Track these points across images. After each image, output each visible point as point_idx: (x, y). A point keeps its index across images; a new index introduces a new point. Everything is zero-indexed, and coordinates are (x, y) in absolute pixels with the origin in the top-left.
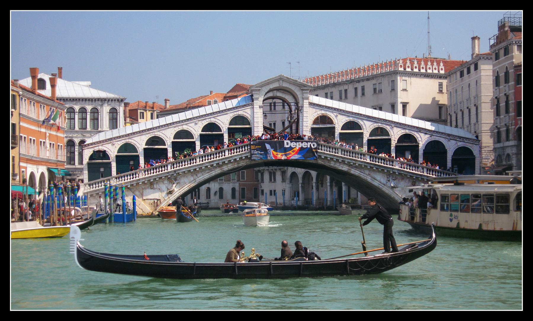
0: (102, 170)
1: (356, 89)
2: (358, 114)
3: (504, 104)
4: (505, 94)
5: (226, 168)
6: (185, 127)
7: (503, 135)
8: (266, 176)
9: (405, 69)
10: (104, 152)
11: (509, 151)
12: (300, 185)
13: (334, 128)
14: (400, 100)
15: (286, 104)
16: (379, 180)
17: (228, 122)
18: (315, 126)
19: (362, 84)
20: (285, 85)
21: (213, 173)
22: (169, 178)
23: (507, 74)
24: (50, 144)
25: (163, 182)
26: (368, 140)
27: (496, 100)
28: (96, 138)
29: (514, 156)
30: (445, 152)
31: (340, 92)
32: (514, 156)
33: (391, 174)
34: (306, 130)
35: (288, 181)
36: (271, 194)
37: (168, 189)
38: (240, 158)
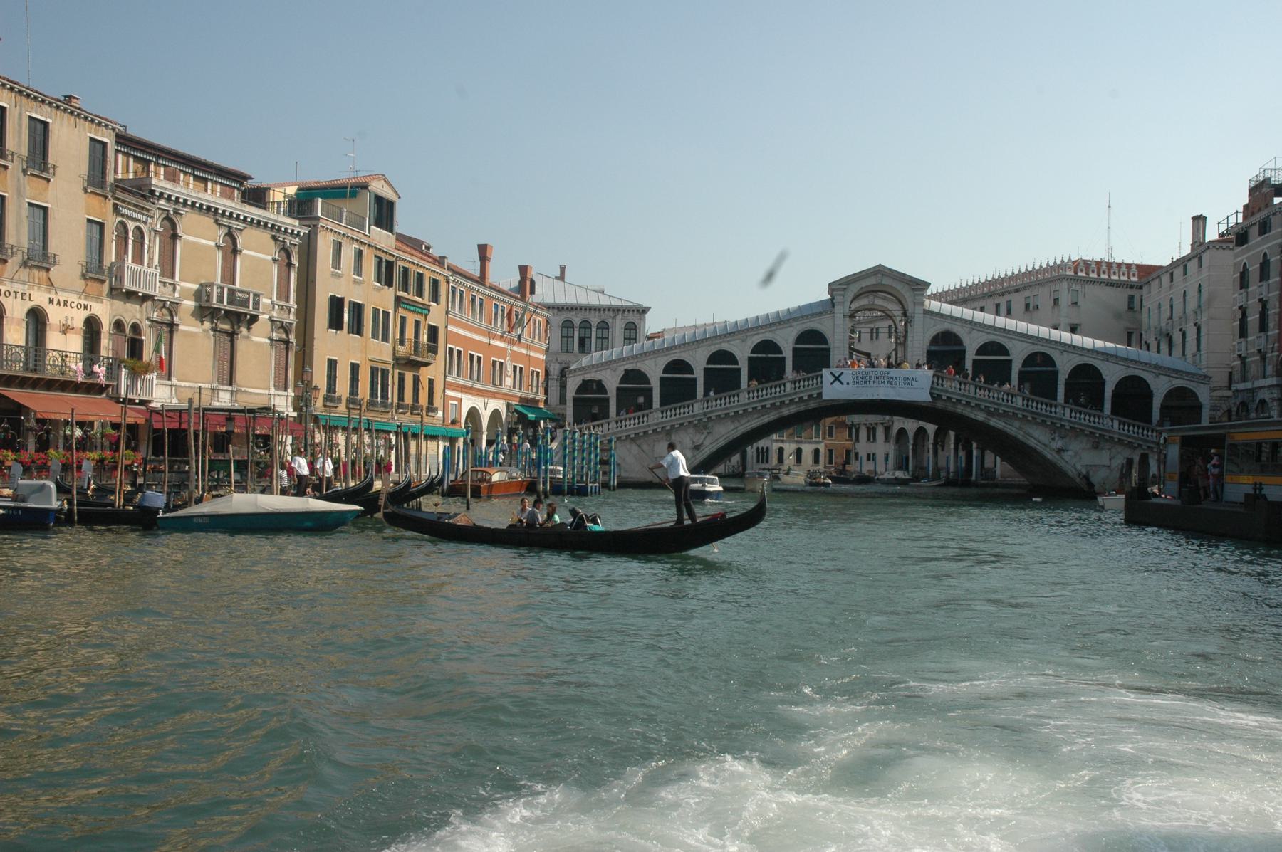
4: (1261, 300)
5: (786, 412)
6: (725, 346)
8: (863, 433)
10: (599, 383)
11: (1265, 395)
16: (1037, 438)
18: (933, 348)
19: (1007, 297)
20: (886, 281)
21: (766, 419)
22: (695, 425)
24: (515, 367)
27: (1240, 312)
28: (584, 361)
30: (1150, 395)
35: (892, 441)
36: (869, 459)
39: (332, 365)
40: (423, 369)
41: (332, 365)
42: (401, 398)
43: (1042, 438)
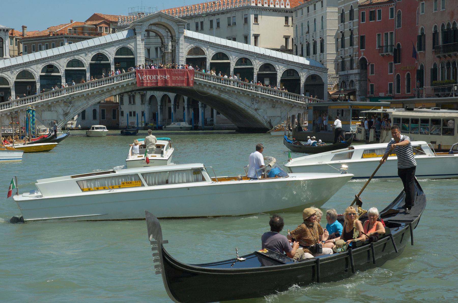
1: (211, 22)
2: (226, 46)
3: (349, 37)
4: (350, 30)
6: (77, 57)
7: (348, 64)
9: (256, 5)
11: (352, 78)
12: (159, 107)
13: (205, 58)
14: (252, 33)
16: (244, 104)
17: (114, 53)
19: (217, 17)
20: (163, 21)
22: (65, 102)
23: (351, 12)
25: (59, 105)
26: (235, 69)
29: (357, 82)
31: (197, 24)
32: (357, 82)
33: (254, 98)
34: (182, 61)
35: (147, 103)
36: (131, 115)
37: (64, 111)
38: (127, 84)
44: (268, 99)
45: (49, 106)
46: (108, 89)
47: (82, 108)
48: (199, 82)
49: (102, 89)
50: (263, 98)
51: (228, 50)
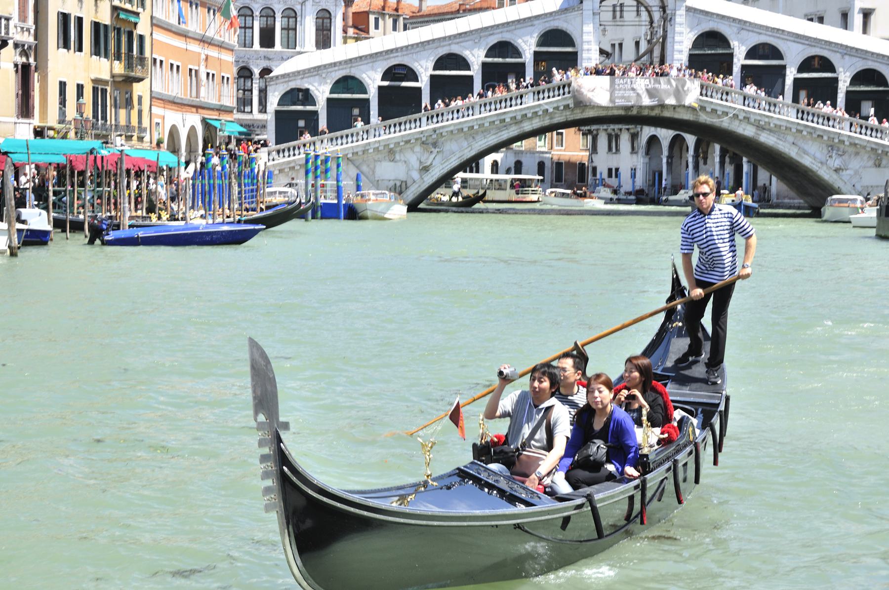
0: (301, 123)
6: (455, 49)
10: (307, 91)
12: (665, 160)
15: (642, 9)
22: (423, 143)
24: (208, 74)
25: (412, 149)
26: (796, 80)
33: (834, 145)
35: (642, 151)
37: (421, 162)
39: (63, 85)
40: (134, 84)
41: (63, 85)
42: (140, 122)
43: (818, 155)
44: (864, 147)
45: (391, 152)
46: (515, 117)
47: (458, 156)
48: (713, 107)
49: (503, 117)
50: (855, 145)
51: (783, 39)
